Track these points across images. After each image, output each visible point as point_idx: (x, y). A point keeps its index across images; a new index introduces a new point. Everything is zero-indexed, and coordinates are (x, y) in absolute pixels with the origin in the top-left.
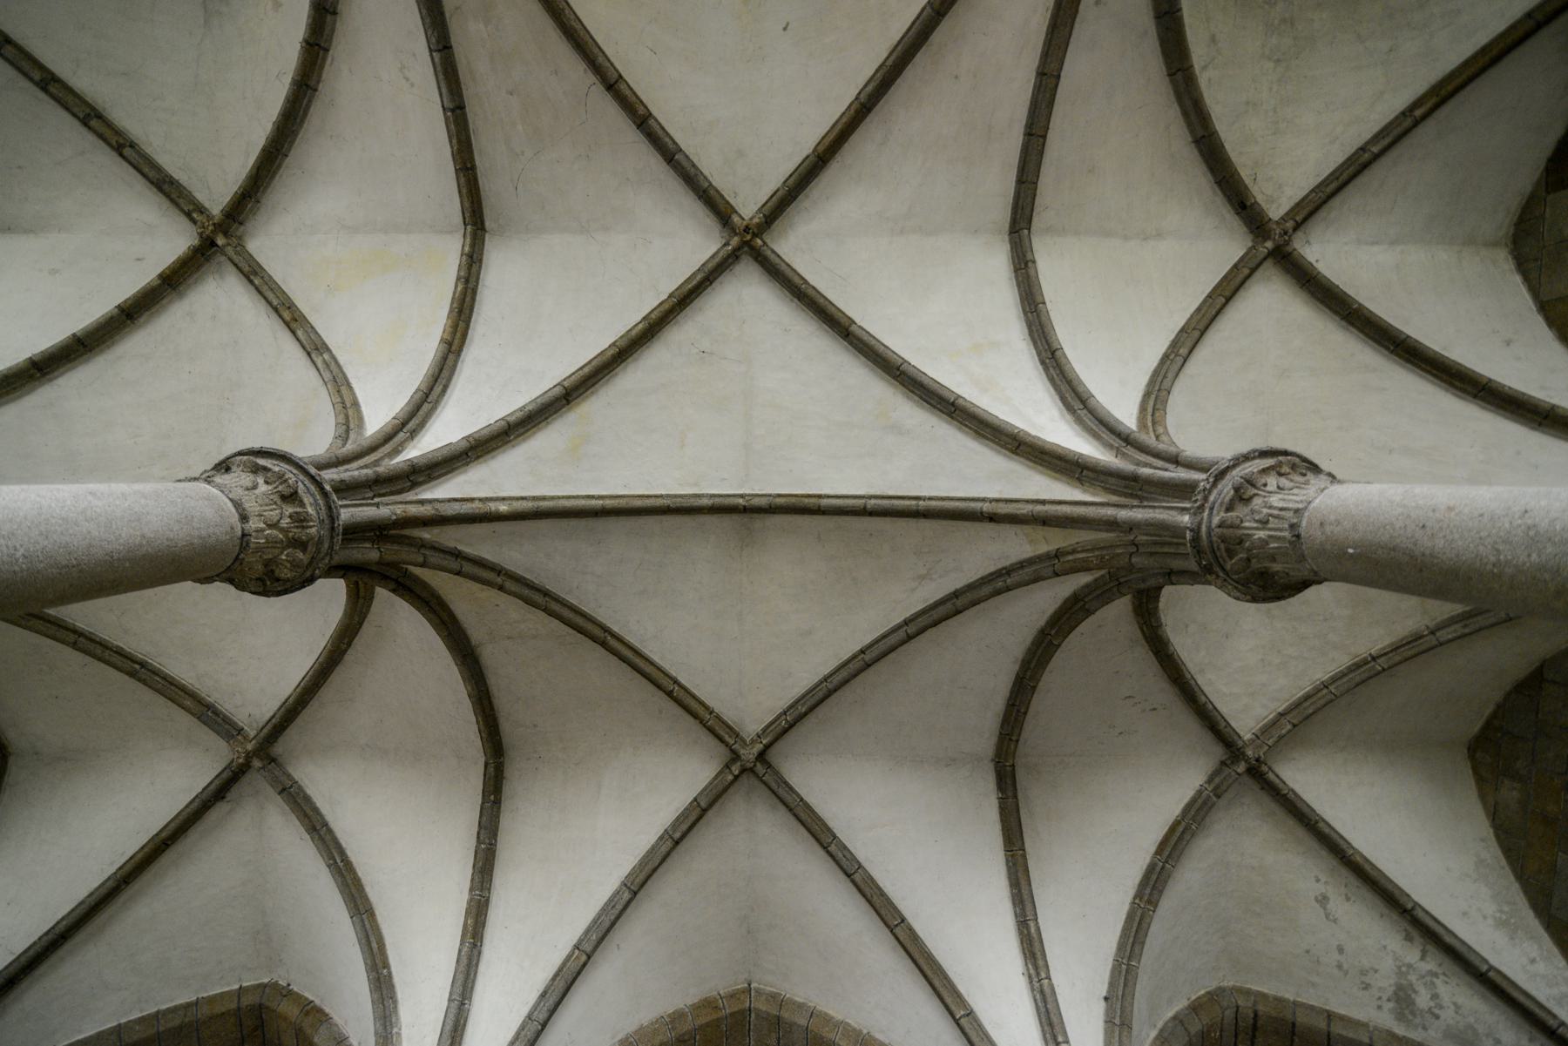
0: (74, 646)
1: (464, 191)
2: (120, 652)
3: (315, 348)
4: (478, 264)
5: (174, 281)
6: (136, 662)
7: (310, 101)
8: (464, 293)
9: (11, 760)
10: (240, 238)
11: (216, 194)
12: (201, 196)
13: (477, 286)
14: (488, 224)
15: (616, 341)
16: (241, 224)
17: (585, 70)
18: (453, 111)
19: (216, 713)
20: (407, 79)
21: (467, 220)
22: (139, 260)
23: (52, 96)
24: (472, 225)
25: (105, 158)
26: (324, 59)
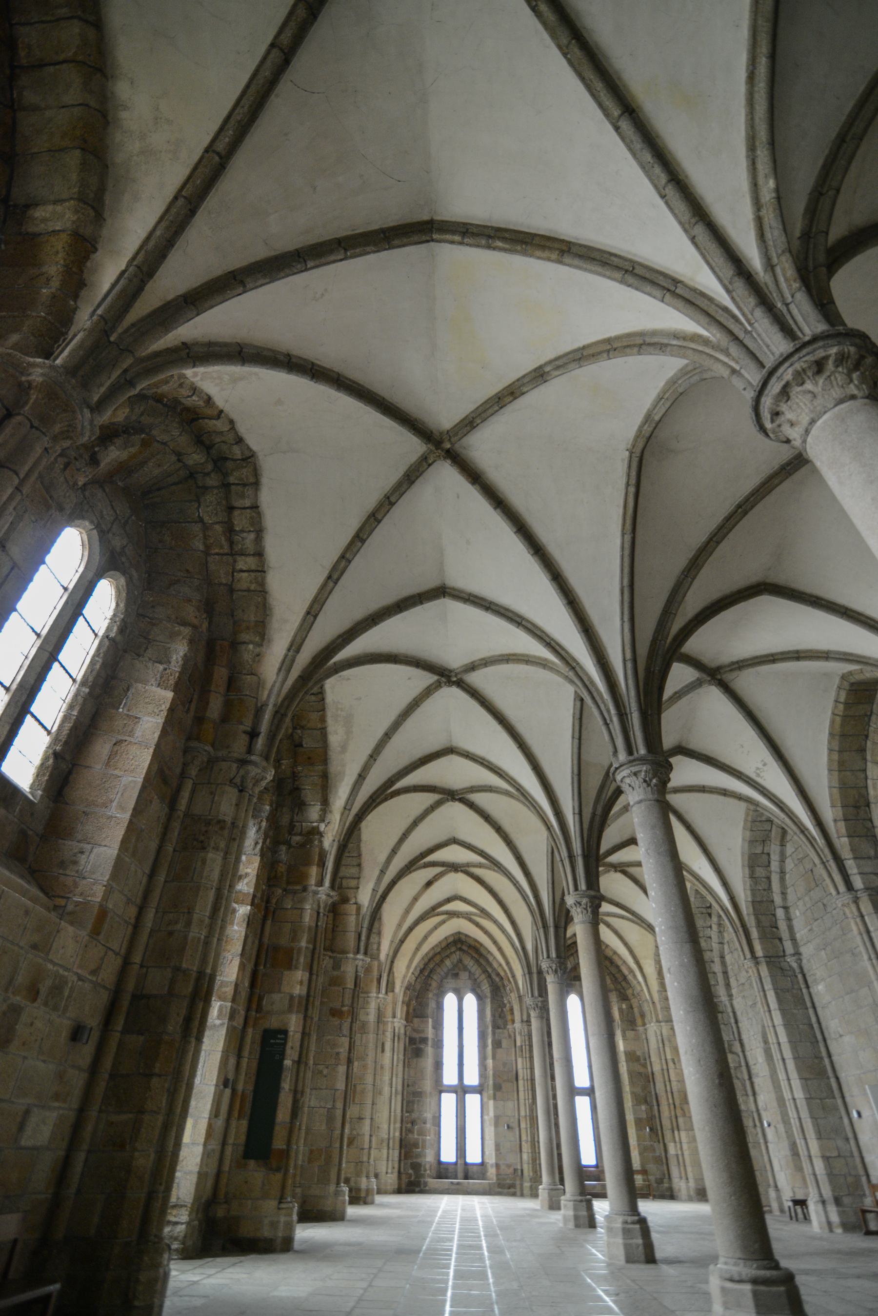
0: (718, 543)
1: (405, 240)
2: (728, 519)
3: (539, 376)
4: (469, 227)
5: (474, 476)
6: (736, 512)
7: (347, 379)
8: (504, 239)
9: (768, 581)
10: (441, 433)
11: (414, 447)
12: (413, 458)
13: (492, 227)
14: (426, 218)
15: (560, 47)
16: (432, 432)
17: (277, 96)
18: (346, 250)
19: (789, 463)
20: (323, 295)
21: (428, 238)
22: (458, 497)
23: (368, 537)
24: (432, 232)
25: (397, 512)
26: (319, 366)
